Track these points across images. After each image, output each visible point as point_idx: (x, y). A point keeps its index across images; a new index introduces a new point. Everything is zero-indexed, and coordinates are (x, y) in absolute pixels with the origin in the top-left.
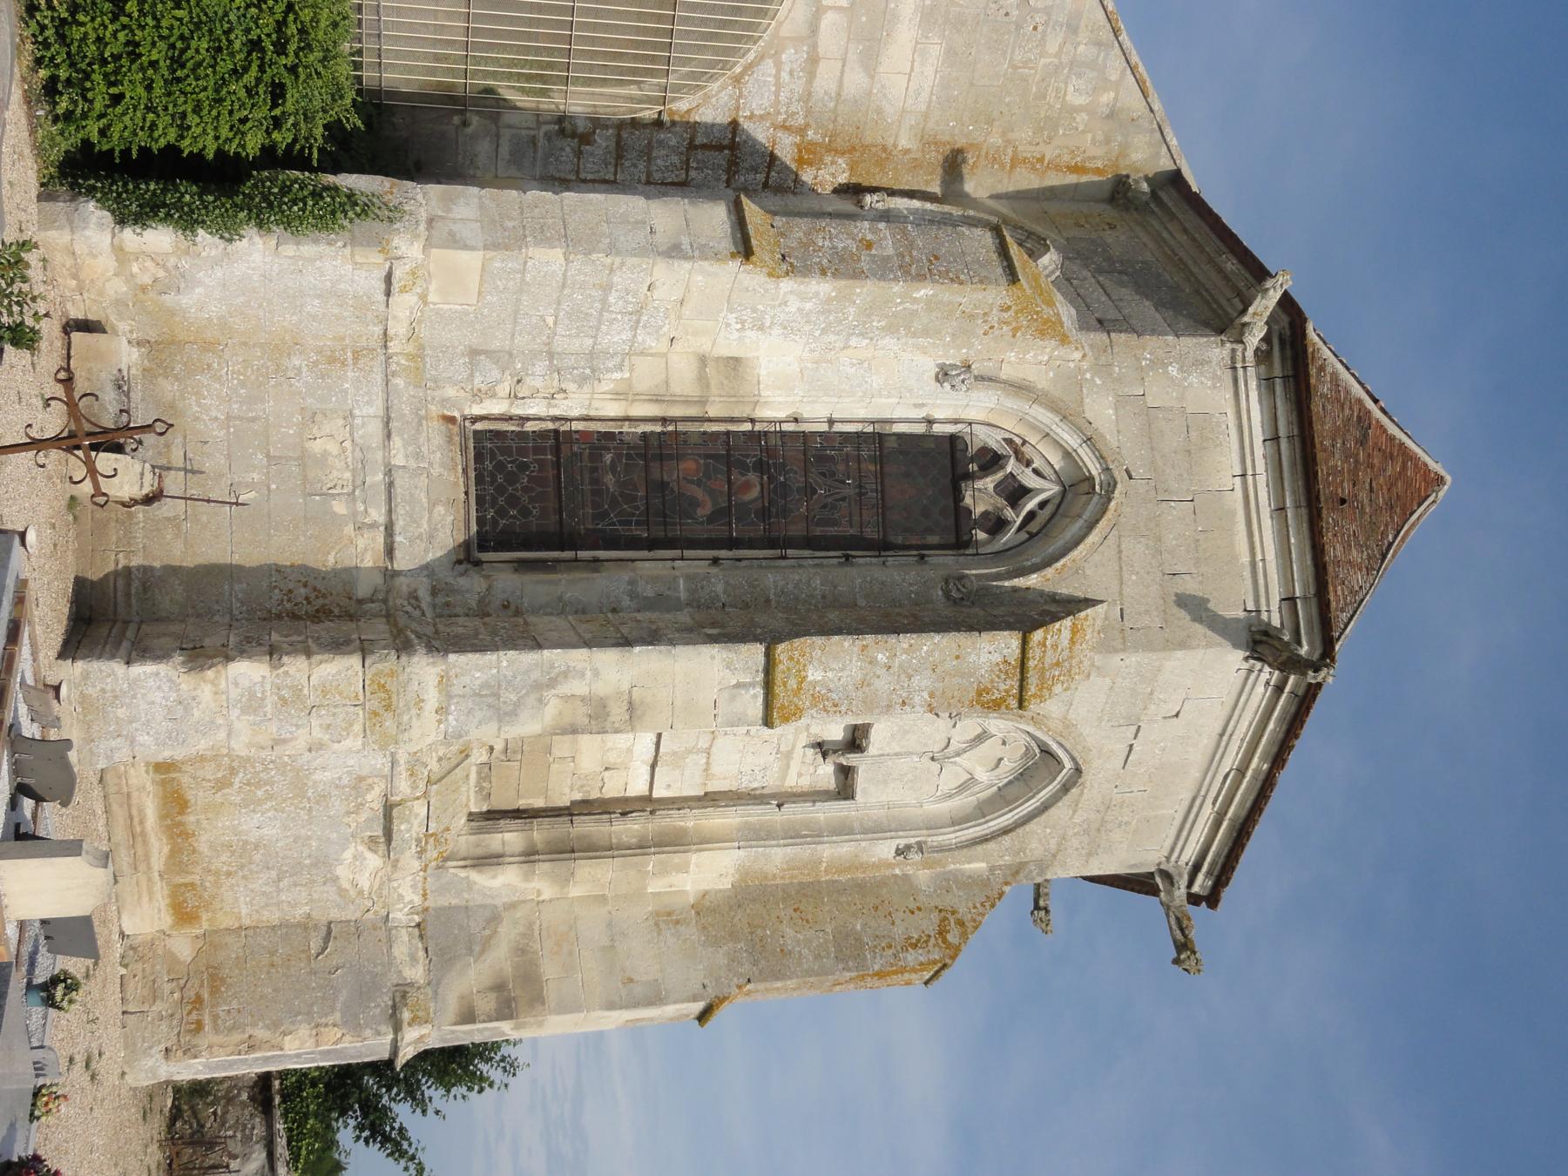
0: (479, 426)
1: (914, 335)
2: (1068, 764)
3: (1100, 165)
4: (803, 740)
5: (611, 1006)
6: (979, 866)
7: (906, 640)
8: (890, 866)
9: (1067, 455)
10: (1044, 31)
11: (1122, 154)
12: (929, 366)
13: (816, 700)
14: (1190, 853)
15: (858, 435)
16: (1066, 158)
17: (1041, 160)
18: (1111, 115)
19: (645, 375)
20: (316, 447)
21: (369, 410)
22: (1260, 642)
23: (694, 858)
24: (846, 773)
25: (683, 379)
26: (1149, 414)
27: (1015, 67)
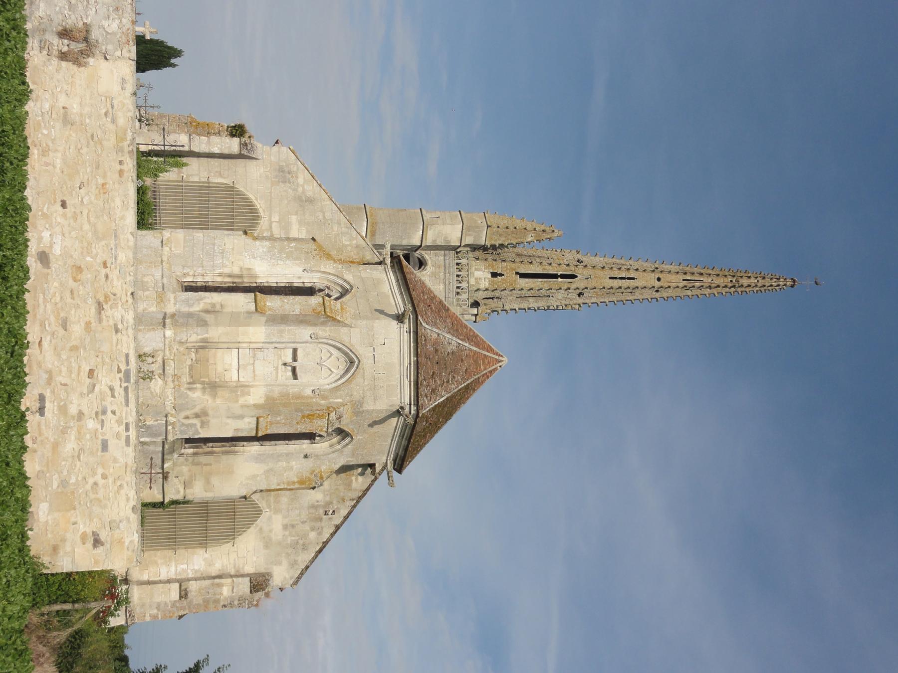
0: (186, 284)
1: (294, 260)
2: (357, 361)
4: (281, 363)
5: (228, 417)
6: (340, 400)
7: (292, 297)
8: (312, 398)
9: (341, 286)
11: (364, 257)
12: (302, 269)
13: (270, 309)
14: (407, 401)
15: (285, 287)
19: (227, 270)
20: (145, 280)
21: (158, 275)
22: (400, 318)
23: (251, 390)
24: (294, 370)
25: (236, 270)
26: (362, 279)
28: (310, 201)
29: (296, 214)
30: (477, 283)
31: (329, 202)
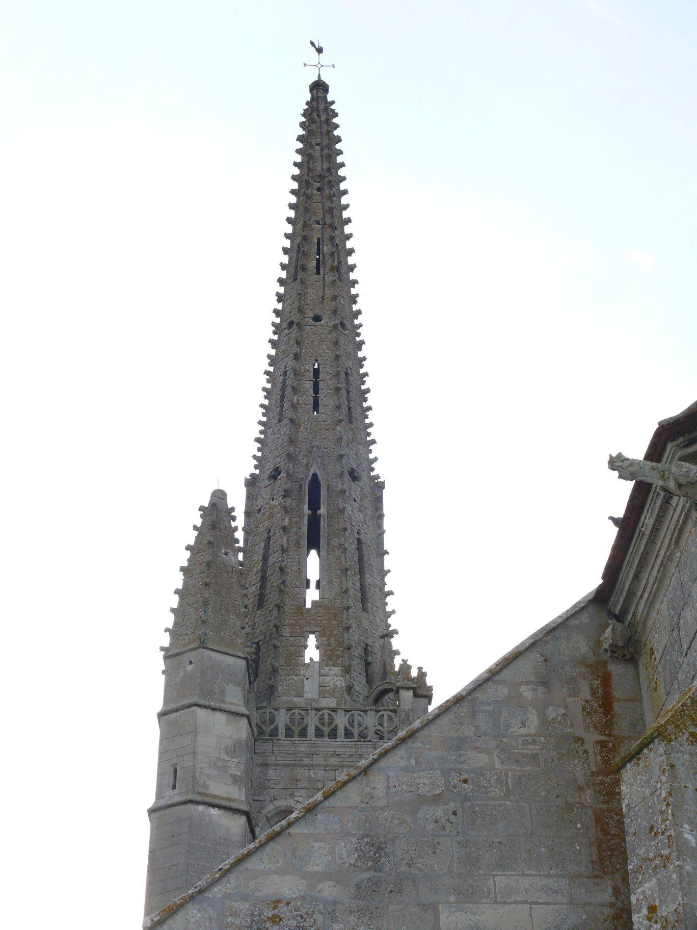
3: (597, 683)
10: (467, 771)
16: (596, 718)
17: (603, 744)
18: (545, 683)
27: (508, 794)
28: (374, 850)
29: (434, 908)
30: (332, 693)
31: (378, 780)
